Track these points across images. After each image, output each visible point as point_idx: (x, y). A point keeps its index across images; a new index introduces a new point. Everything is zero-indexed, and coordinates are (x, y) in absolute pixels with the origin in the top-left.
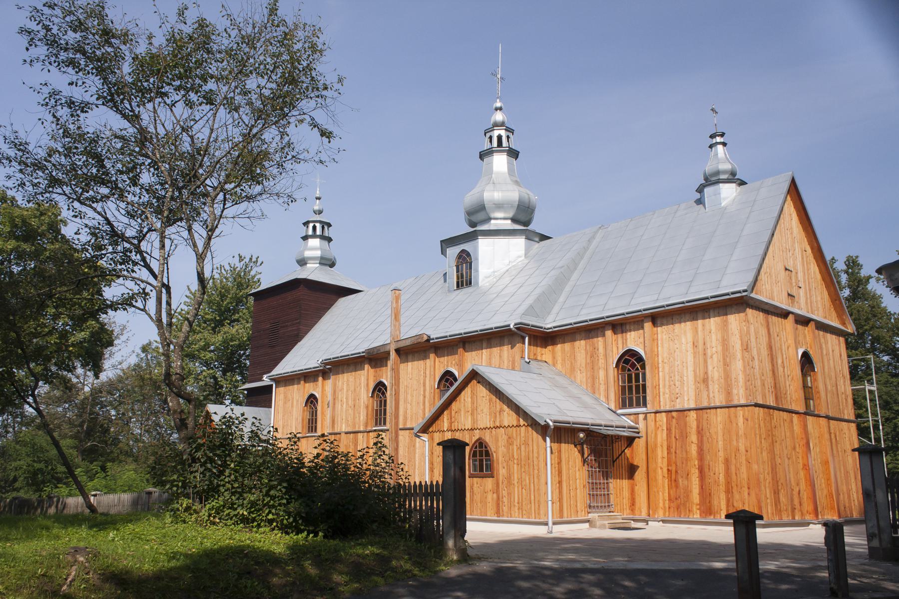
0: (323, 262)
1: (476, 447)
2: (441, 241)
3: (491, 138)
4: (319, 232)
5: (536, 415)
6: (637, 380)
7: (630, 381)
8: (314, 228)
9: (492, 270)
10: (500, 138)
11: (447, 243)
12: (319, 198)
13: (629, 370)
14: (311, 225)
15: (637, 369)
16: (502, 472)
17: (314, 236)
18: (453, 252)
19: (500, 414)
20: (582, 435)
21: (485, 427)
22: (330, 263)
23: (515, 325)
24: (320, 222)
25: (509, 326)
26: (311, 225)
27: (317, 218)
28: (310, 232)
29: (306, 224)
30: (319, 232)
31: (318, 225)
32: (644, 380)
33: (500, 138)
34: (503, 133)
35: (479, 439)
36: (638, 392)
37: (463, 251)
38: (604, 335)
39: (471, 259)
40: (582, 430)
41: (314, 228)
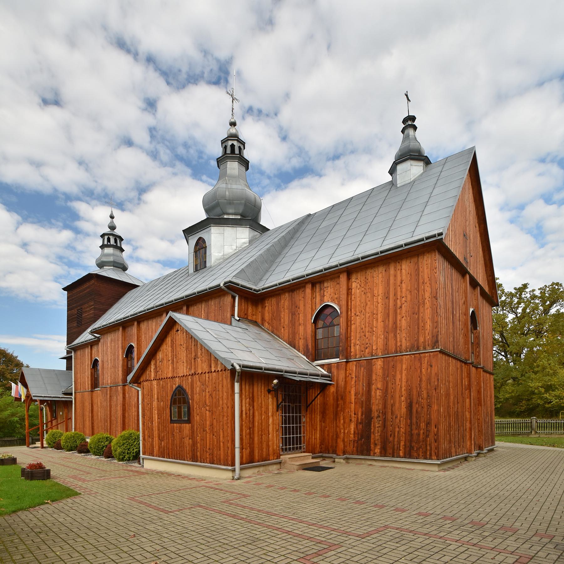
1: (176, 396)
2: (183, 231)
8: (109, 240)
11: (188, 232)
14: (106, 237)
16: (197, 418)
19: (195, 362)
20: (275, 381)
21: (182, 375)
22: (121, 266)
23: (225, 283)
25: (219, 285)
26: (106, 237)
28: (106, 243)
29: (103, 236)
30: (112, 242)
31: (111, 237)
35: (179, 386)
38: (304, 291)
40: (277, 377)
41: (109, 240)
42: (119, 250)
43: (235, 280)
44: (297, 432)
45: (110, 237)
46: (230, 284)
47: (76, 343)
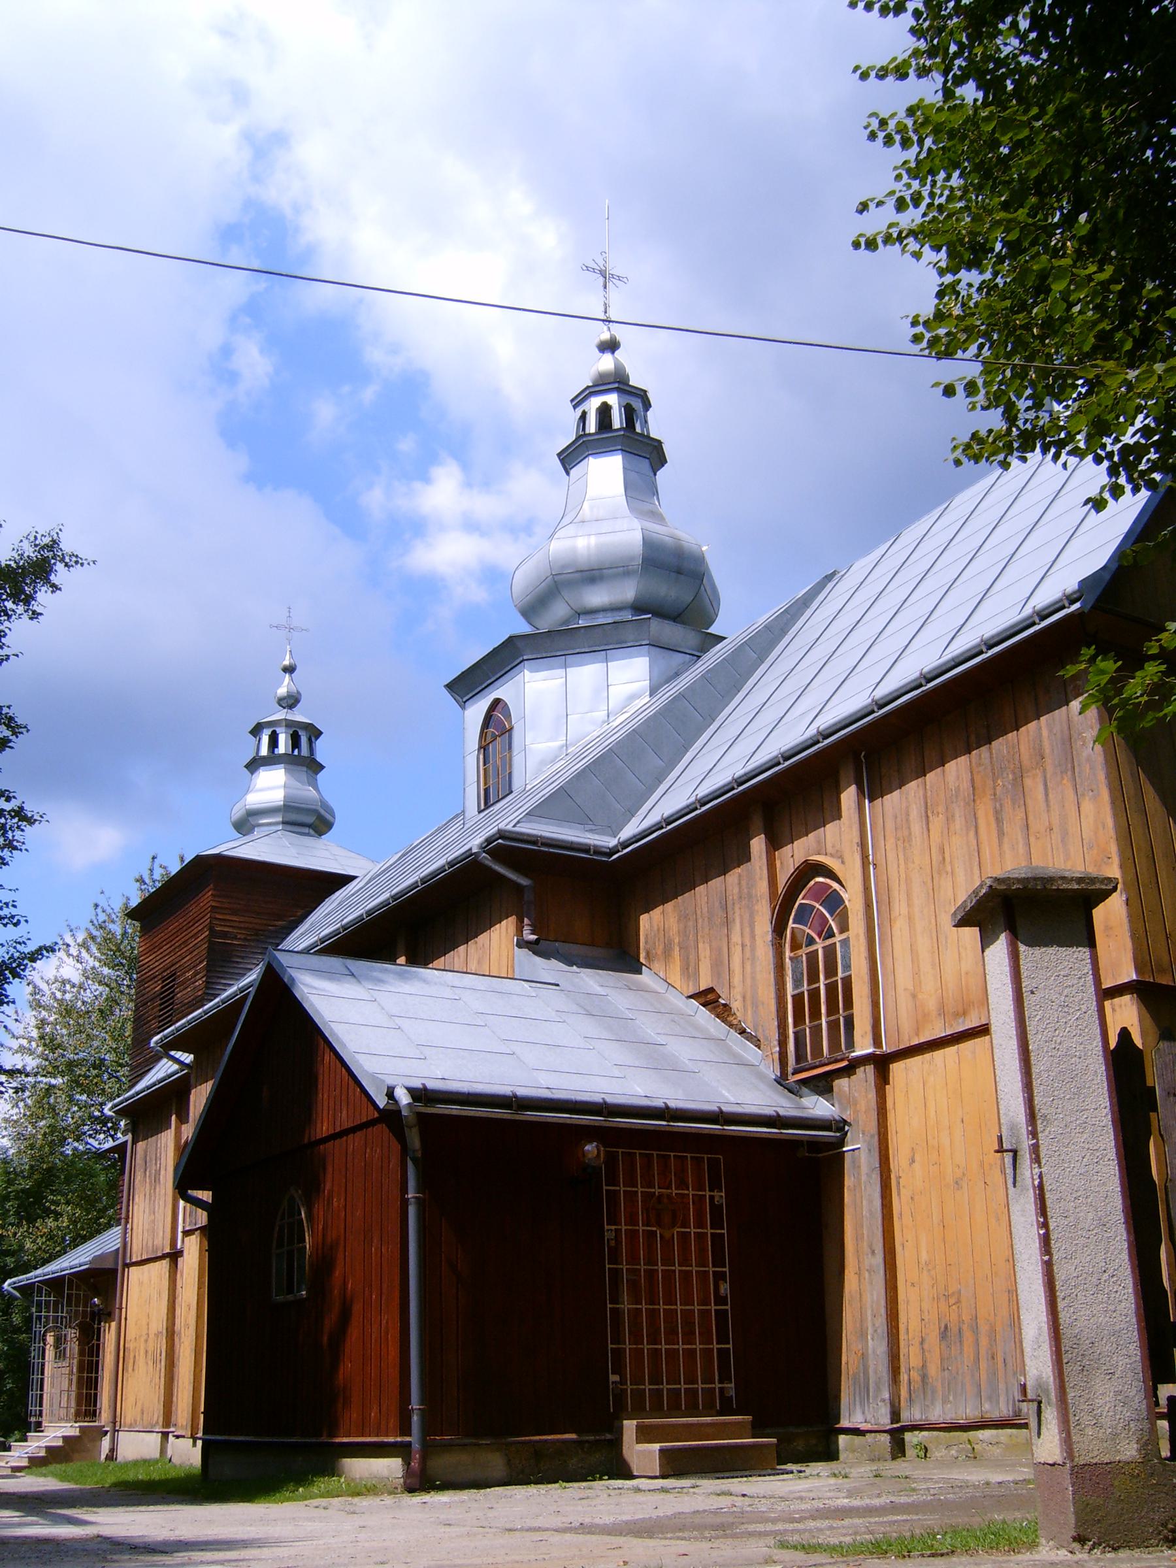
0: (293, 817)
3: (583, 417)
4: (283, 747)
5: (373, 1077)
6: (831, 971)
7: (813, 977)
8: (274, 741)
9: (561, 742)
10: (605, 410)
12: (289, 670)
13: (811, 941)
15: (831, 935)
17: (271, 760)
18: (478, 710)
24: (289, 724)
27: (281, 715)
28: (264, 751)
30: (283, 747)
32: (847, 967)
33: (605, 410)
34: (612, 399)
36: (832, 1009)
37: (497, 702)
39: (510, 721)
41: (274, 741)
42: (305, 769)
43: (527, 829)
44: (672, 1333)
45: (278, 730)
46: (500, 841)
47: (154, 1080)
